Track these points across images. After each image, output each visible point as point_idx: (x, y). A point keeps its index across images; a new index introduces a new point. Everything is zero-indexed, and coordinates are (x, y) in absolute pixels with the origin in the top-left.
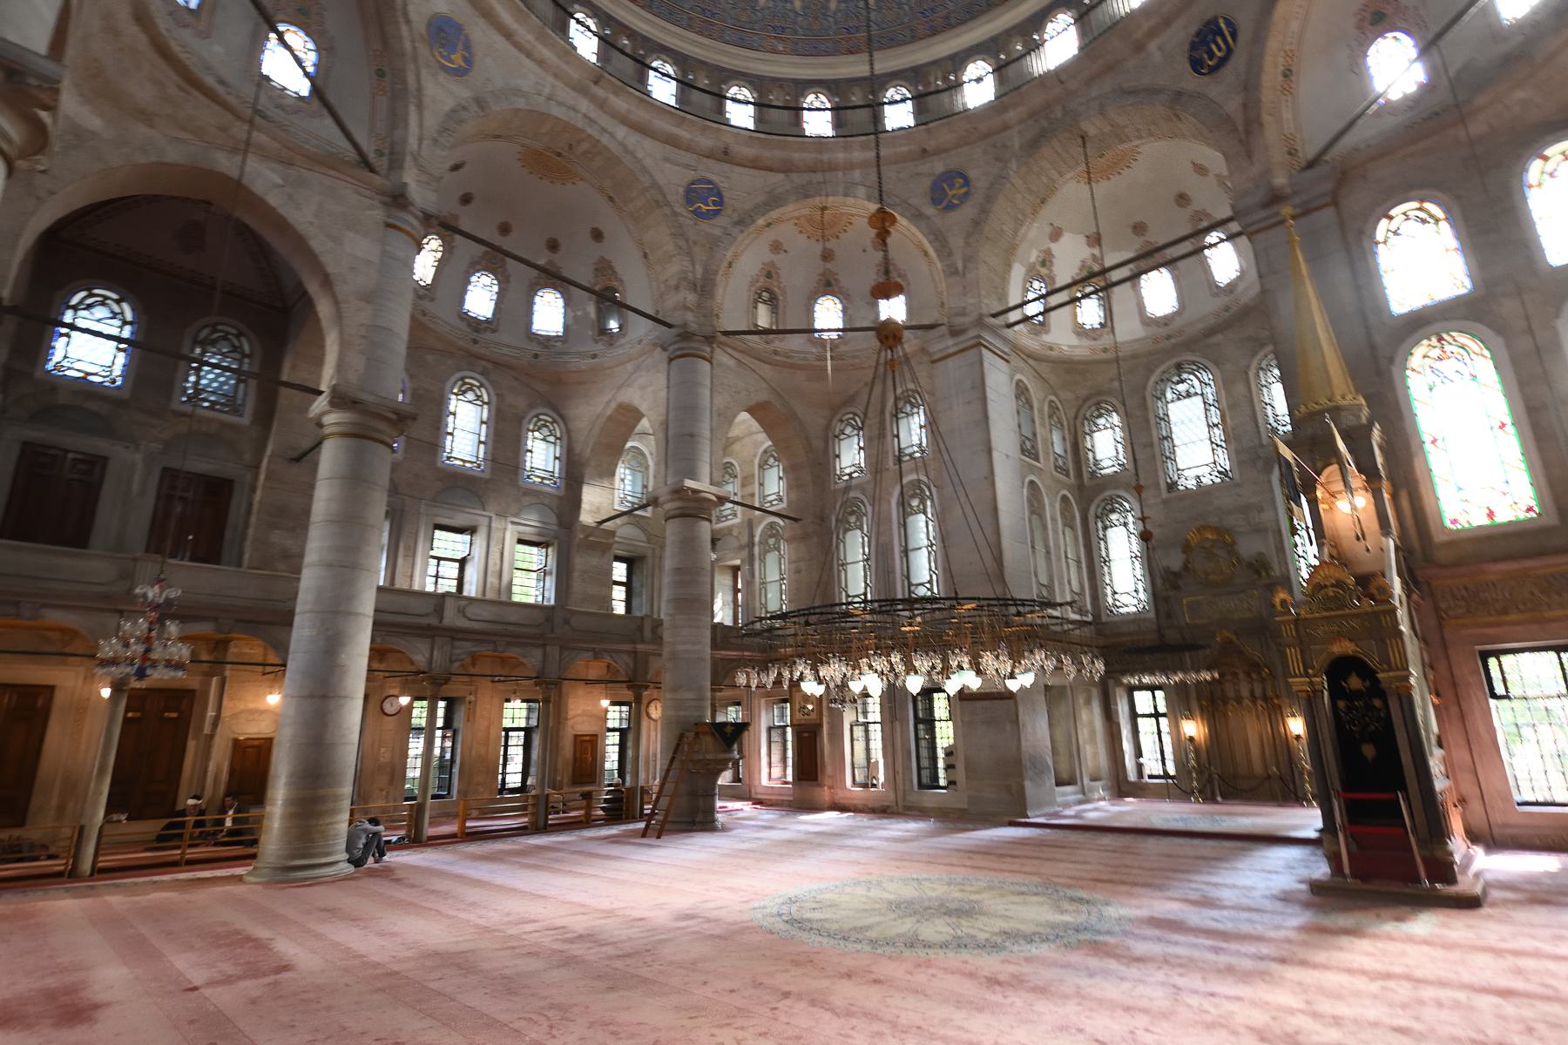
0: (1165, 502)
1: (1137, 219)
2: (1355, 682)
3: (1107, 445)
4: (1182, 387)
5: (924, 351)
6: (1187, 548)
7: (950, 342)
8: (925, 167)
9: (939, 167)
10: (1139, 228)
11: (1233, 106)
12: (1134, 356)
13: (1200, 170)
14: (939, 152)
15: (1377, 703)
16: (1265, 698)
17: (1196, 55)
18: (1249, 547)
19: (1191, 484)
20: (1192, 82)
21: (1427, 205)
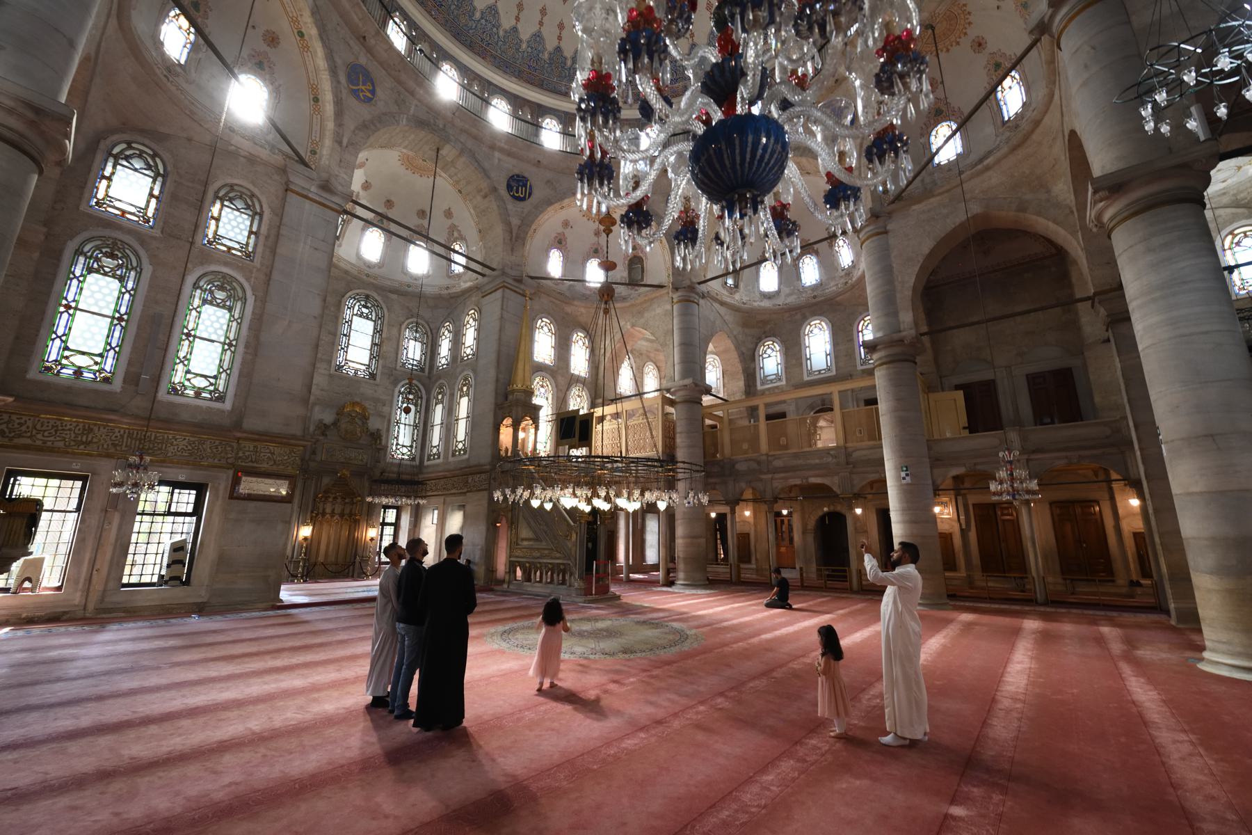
0: (331, 376)
1: (393, 199)
4: (364, 310)
5: (283, 171)
6: (340, 413)
7: (313, 189)
8: (356, 47)
9: (363, 60)
10: (389, 204)
11: (515, 221)
12: (346, 272)
13: (448, 214)
14: (369, 51)
16: (342, 515)
17: (513, 184)
18: (374, 424)
19: (352, 373)
20: (503, 191)
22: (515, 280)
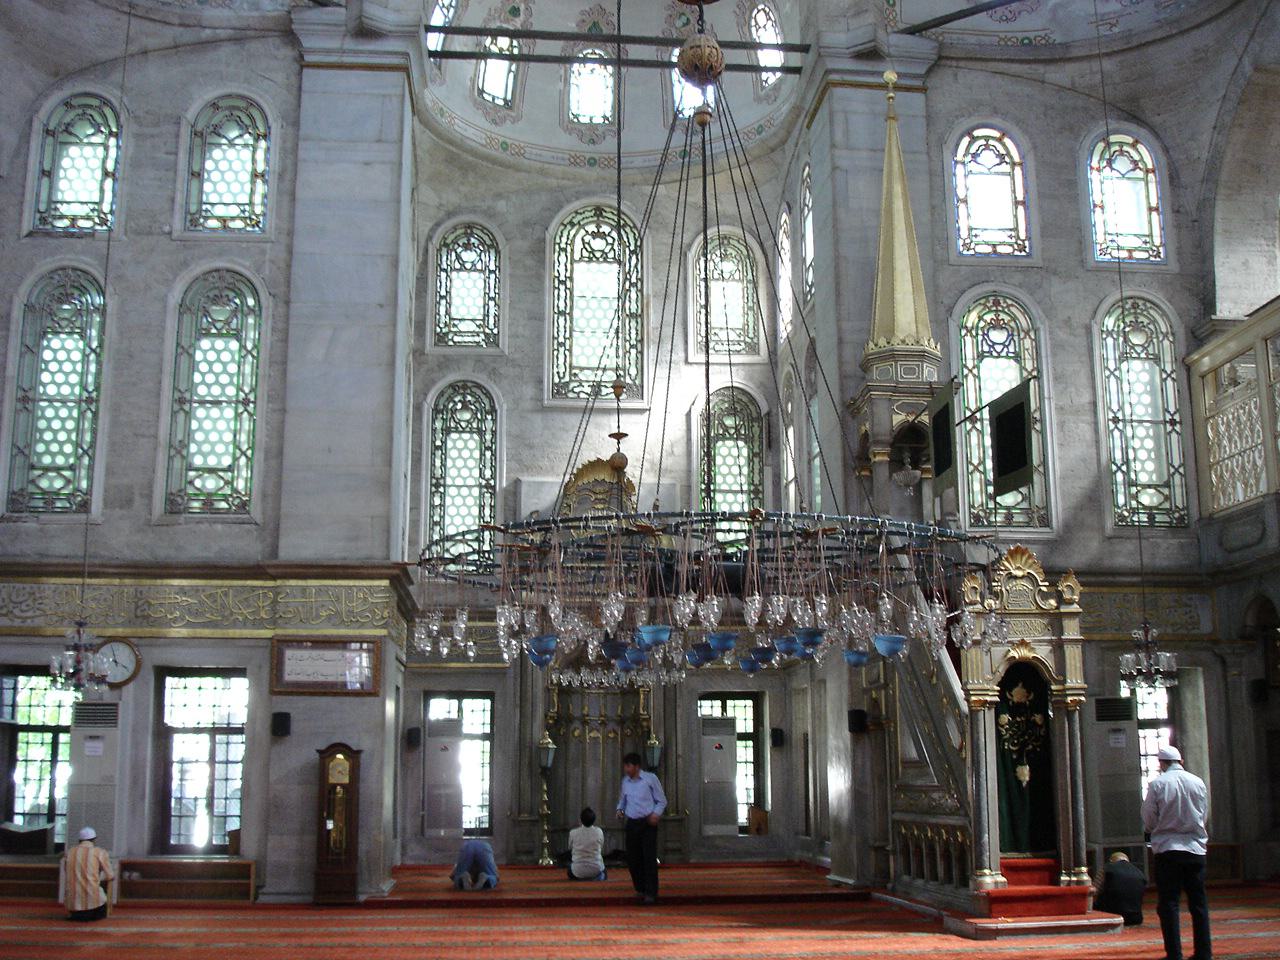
2: (1018, 694)
3: (467, 295)
4: (598, 244)
7: (350, 44)
15: (1038, 718)
21: (1007, 140)
22: (859, 56)
